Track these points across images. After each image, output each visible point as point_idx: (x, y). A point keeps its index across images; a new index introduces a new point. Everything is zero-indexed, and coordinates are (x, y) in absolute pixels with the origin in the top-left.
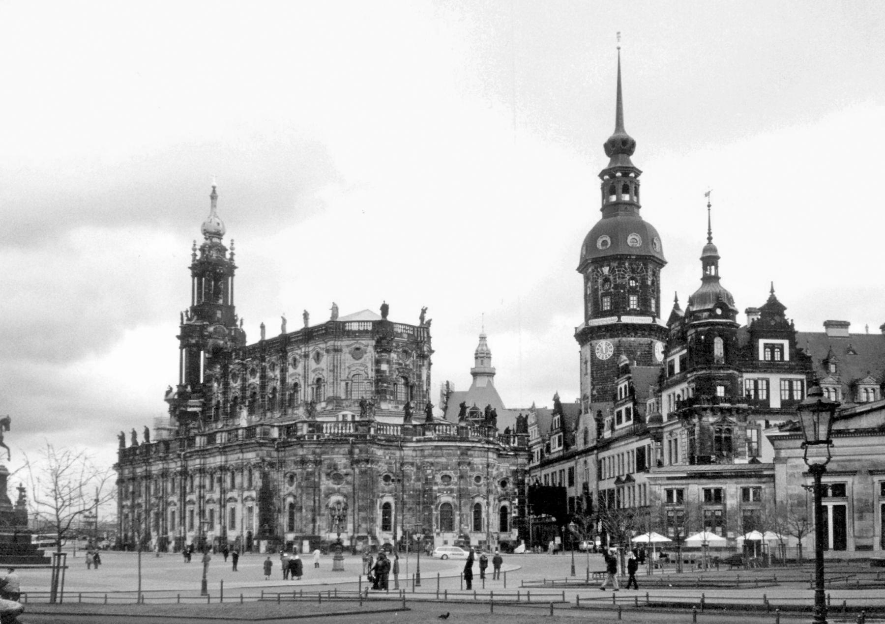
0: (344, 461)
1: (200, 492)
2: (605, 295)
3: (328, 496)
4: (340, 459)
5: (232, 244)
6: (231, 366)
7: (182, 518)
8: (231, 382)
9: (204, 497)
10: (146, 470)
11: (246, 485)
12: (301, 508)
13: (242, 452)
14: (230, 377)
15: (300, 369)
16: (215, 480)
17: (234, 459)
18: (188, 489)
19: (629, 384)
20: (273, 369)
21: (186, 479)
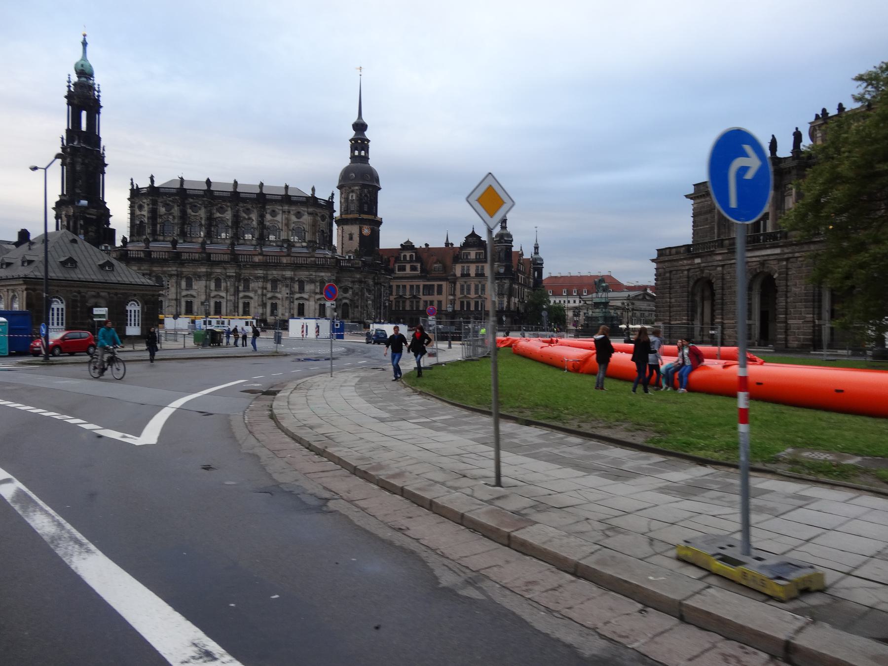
0: (372, 283)
1: (263, 291)
2: (366, 203)
3: (367, 301)
4: (371, 282)
5: (99, 88)
6: (191, 200)
7: (236, 307)
8: (189, 211)
9: (266, 295)
10: (177, 271)
11: (318, 290)
12: (357, 307)
13: (316, 272)
14: (188, 206)
15: (279, 218)
16: (280, 286)
17: (303, 274)
18: (241, 288)
19: (416, 254)
20: (248, 211)
21: (239, 281)
